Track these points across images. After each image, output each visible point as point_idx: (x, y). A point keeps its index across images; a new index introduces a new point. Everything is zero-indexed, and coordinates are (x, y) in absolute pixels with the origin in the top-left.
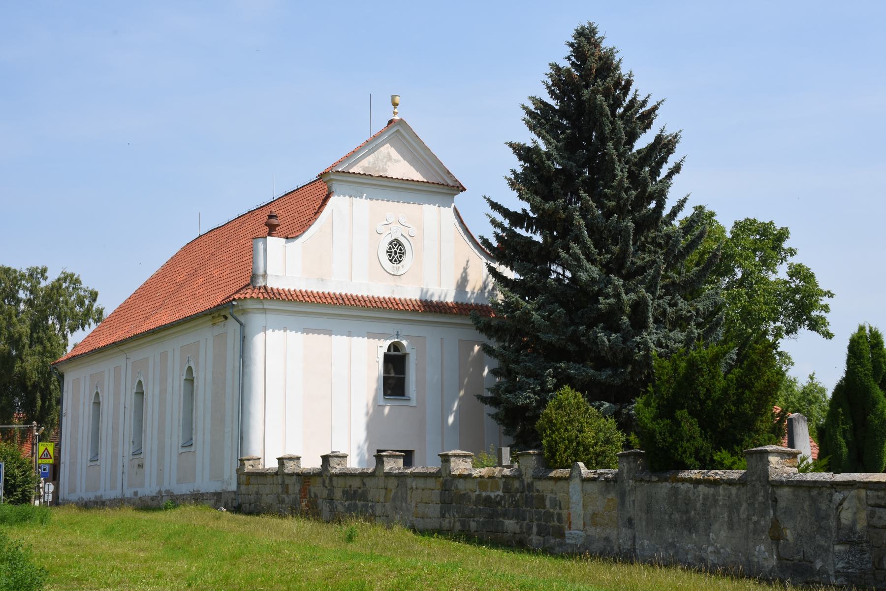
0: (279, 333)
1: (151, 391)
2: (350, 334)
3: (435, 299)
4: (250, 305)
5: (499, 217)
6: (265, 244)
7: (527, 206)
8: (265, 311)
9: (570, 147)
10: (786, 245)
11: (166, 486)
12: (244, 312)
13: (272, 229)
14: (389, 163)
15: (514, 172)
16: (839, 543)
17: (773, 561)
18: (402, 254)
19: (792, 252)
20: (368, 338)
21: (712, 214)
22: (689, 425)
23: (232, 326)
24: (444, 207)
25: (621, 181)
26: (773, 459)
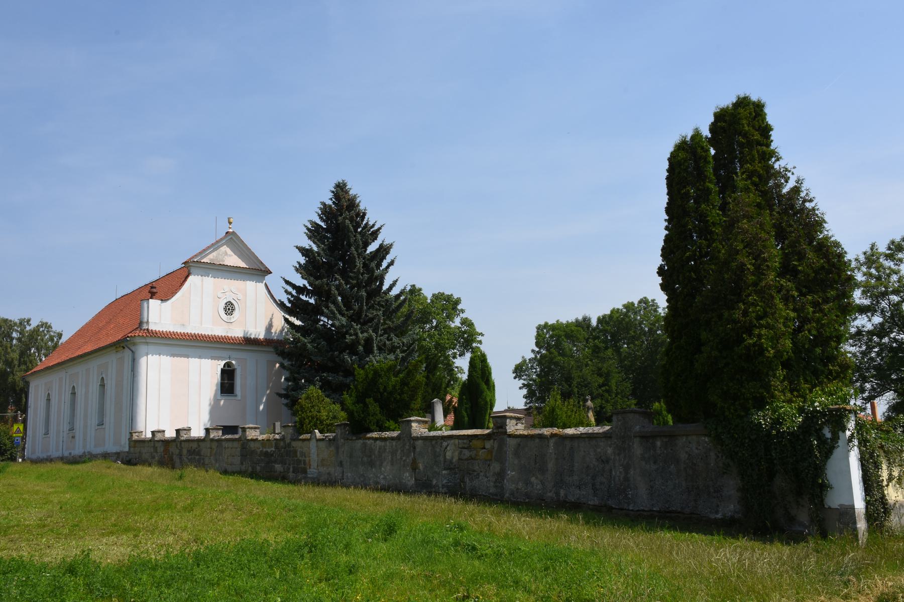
0: (156, 357)
1: (80, 392)
2: (200, 357)
3: (252, 337)
4: (138, 340)
5: (290, 289)
6: (148, 304)
7: (305, 282)
8: (147, 343)
9: (331, 249)
10: (459, 307)
11: (88, 449)
12: (134, 344)
13: (153, 295)
15: (299, 263)
16: (445, 469)
17: (413, 482)
18: (233, 310)
19: (463, 311)
21: (420, 290)
22: (374, 407)
23: (127, 353)
25: (359, 269)
26: (414, 425)
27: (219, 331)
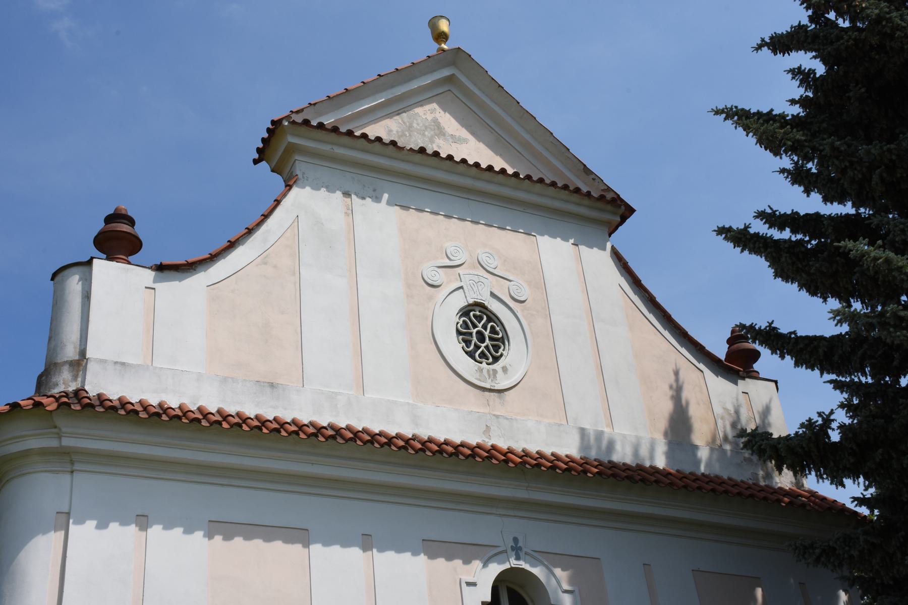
0: (122, 536)
2: (367, 543)
6: (87, 281)
8: (67, 459)
20: (432, 556)
24: (591, 246)
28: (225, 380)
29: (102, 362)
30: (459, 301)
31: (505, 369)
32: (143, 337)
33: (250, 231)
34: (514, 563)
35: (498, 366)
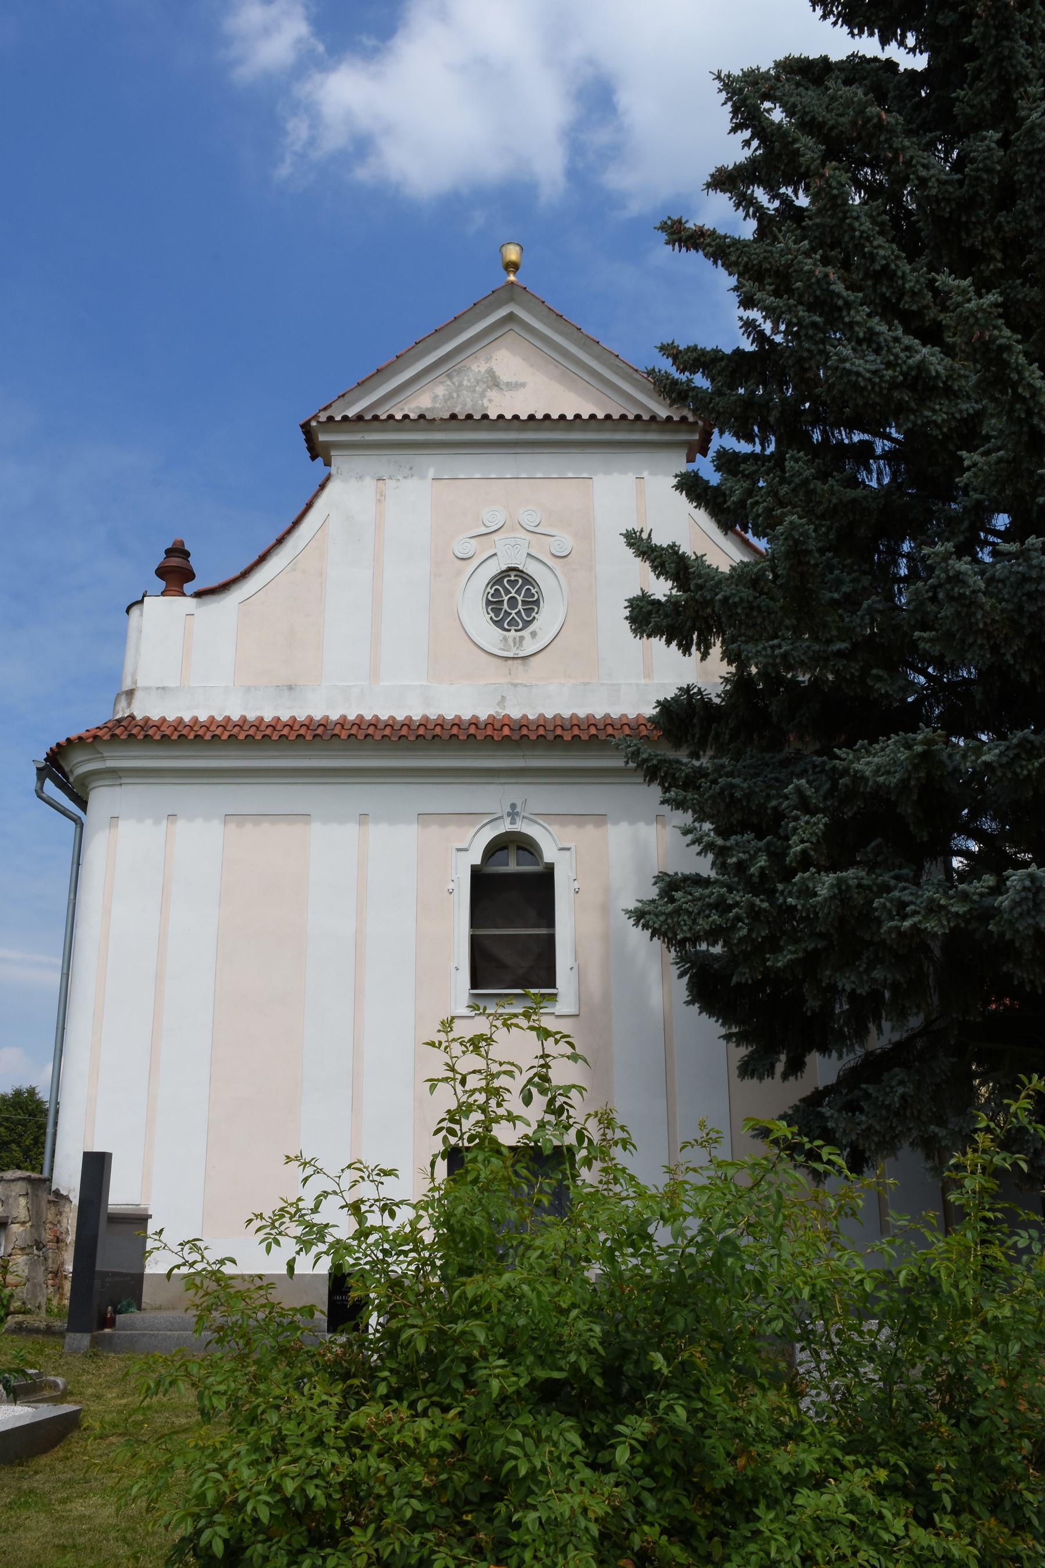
8: (115, 774)
14: (492, 394)
18: (533, 604)
27: (463, 698)
28: (248, 689)
29: (147, 689)
30: (493, 569)
31: (534, 634)
32: (186, 660)
33: (280, 541)
34: (505, 826)
35: (526, 633)
